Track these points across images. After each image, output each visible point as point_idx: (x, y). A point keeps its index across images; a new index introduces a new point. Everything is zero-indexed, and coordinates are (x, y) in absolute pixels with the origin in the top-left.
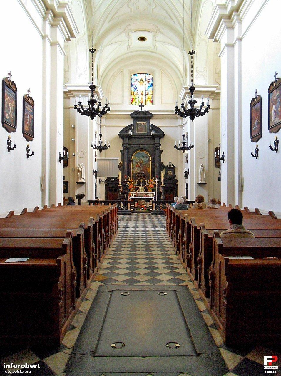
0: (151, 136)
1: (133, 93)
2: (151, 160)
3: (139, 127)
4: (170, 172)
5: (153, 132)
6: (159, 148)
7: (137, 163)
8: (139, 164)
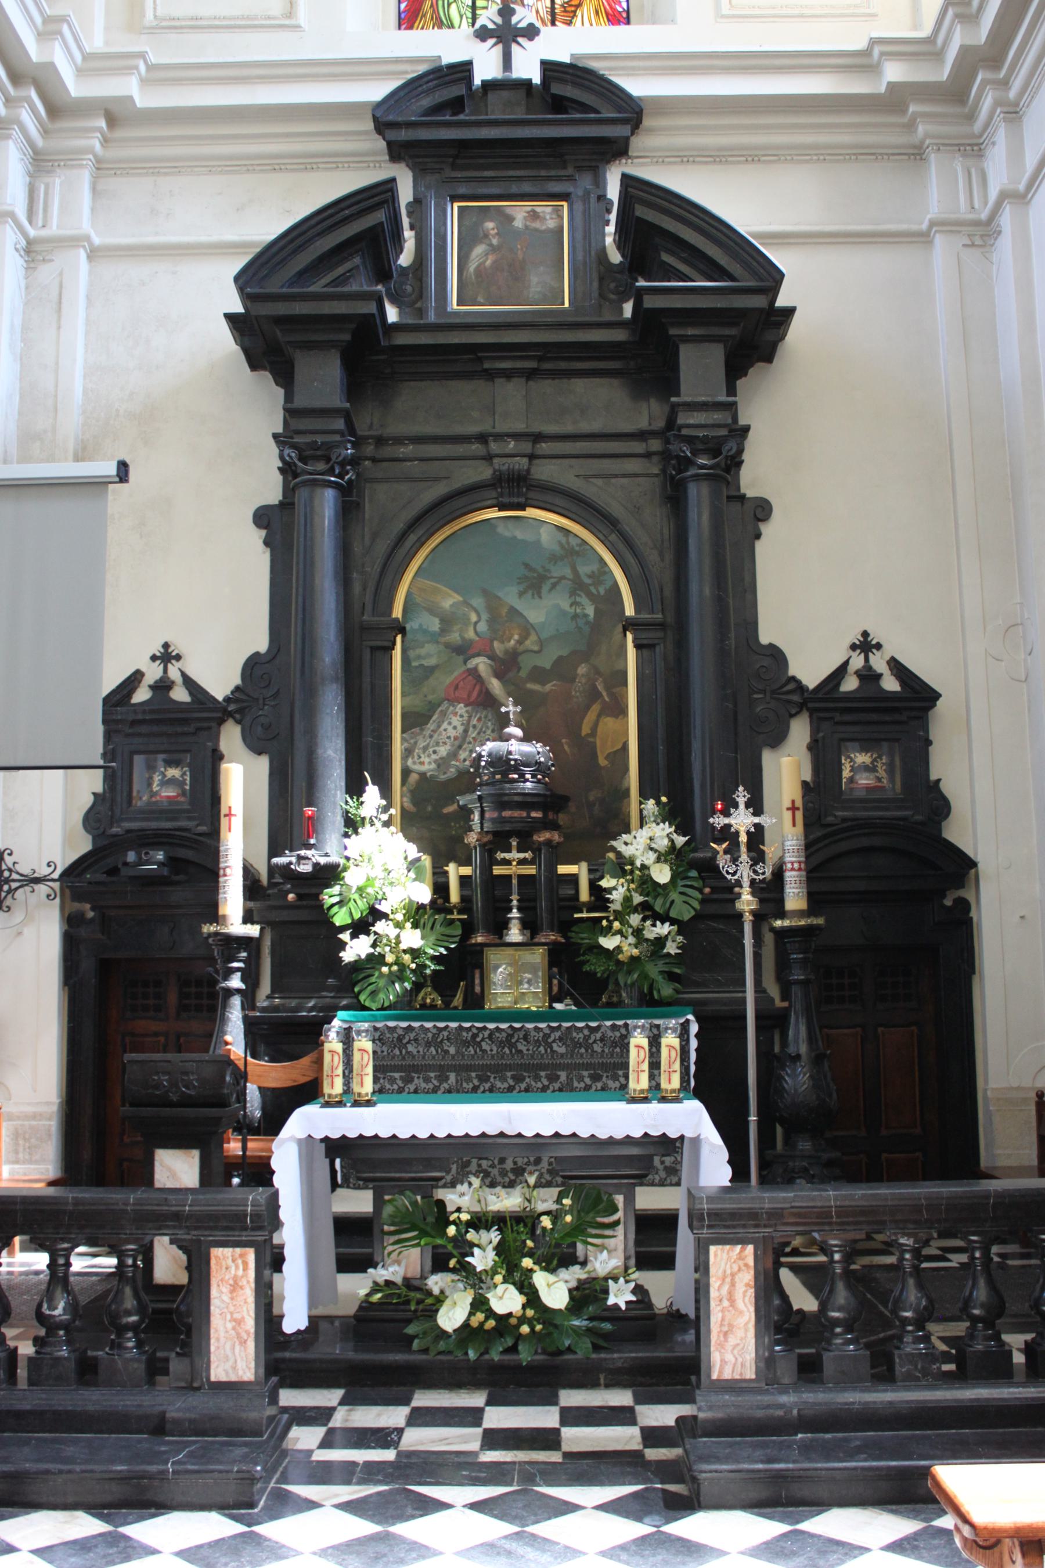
0: (619, 335)
2: (629, 611)
3: (479, 250)
7: (464, 650)
8: (481, 664)
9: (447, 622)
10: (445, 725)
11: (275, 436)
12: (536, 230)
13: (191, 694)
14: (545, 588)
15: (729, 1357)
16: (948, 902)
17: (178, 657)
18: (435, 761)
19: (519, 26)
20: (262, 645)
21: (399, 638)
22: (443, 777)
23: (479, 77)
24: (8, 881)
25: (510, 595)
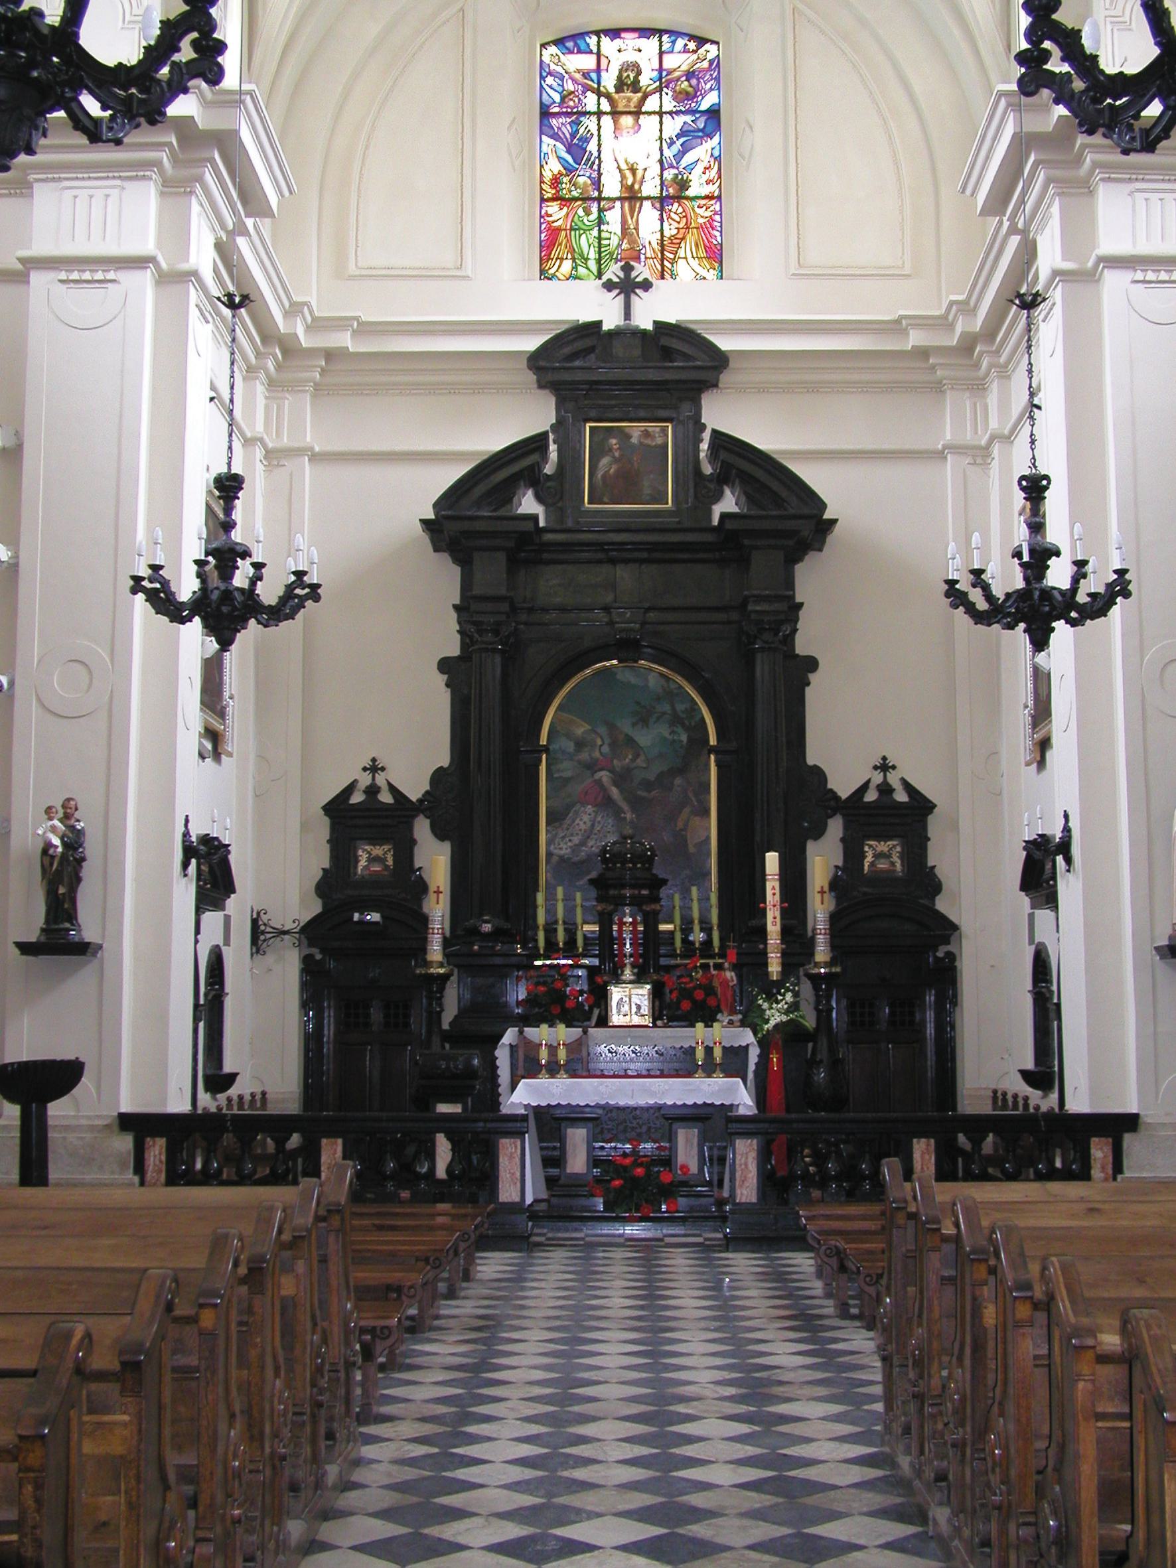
0: (709, 538)
1: (556, 181)
2: (713, 741)
3: (605, 461)
4: (883, 847)
5: (728, 503)
6: (789, 640)
7: (592, 767)
8: (604, 776)
9: (580, 745)
10: (577, 821)
11: (455, 607)
12: (649, 446)
13: (394, 797)
14: (652, 720)
15: (745, 1192)
16: (940, 954)
17: (383, 769)
18: (571, 847)
19: (637, 280)
20: (444, 760)
21: (544, 756)
22: (576, 859)
23: (606, 327)
24: (263, 933)
25: (625, 726)
